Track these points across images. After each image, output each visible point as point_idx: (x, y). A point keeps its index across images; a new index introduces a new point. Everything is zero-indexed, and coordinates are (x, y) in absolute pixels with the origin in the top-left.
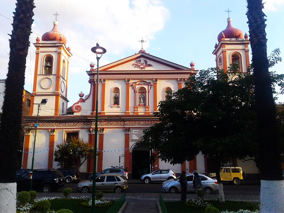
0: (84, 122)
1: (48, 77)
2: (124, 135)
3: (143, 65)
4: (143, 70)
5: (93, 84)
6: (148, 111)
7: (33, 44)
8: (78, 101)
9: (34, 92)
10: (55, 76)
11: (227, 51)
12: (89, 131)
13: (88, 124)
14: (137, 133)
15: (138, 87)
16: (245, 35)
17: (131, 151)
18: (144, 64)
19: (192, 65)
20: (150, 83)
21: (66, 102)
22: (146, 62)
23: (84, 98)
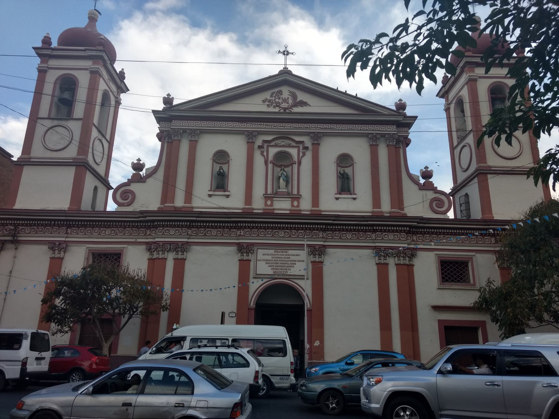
1: (63, 123)
2: (238, 263)
4: (287, 111)
5: (167, 142)
6: (298, 206)
7: (34, 48)
8: (128, 180)
9: (24, 156)
10: (80, 123)
11: (478, 79)
12: (149, 250)
13: (148, 233)
14: (269, 257)
15: (273, 151)
17: (252, 304)
18: (290, 101)
20: (302, 142)
21: (105, 189)
22: (294, 96)
23: (143, 173)
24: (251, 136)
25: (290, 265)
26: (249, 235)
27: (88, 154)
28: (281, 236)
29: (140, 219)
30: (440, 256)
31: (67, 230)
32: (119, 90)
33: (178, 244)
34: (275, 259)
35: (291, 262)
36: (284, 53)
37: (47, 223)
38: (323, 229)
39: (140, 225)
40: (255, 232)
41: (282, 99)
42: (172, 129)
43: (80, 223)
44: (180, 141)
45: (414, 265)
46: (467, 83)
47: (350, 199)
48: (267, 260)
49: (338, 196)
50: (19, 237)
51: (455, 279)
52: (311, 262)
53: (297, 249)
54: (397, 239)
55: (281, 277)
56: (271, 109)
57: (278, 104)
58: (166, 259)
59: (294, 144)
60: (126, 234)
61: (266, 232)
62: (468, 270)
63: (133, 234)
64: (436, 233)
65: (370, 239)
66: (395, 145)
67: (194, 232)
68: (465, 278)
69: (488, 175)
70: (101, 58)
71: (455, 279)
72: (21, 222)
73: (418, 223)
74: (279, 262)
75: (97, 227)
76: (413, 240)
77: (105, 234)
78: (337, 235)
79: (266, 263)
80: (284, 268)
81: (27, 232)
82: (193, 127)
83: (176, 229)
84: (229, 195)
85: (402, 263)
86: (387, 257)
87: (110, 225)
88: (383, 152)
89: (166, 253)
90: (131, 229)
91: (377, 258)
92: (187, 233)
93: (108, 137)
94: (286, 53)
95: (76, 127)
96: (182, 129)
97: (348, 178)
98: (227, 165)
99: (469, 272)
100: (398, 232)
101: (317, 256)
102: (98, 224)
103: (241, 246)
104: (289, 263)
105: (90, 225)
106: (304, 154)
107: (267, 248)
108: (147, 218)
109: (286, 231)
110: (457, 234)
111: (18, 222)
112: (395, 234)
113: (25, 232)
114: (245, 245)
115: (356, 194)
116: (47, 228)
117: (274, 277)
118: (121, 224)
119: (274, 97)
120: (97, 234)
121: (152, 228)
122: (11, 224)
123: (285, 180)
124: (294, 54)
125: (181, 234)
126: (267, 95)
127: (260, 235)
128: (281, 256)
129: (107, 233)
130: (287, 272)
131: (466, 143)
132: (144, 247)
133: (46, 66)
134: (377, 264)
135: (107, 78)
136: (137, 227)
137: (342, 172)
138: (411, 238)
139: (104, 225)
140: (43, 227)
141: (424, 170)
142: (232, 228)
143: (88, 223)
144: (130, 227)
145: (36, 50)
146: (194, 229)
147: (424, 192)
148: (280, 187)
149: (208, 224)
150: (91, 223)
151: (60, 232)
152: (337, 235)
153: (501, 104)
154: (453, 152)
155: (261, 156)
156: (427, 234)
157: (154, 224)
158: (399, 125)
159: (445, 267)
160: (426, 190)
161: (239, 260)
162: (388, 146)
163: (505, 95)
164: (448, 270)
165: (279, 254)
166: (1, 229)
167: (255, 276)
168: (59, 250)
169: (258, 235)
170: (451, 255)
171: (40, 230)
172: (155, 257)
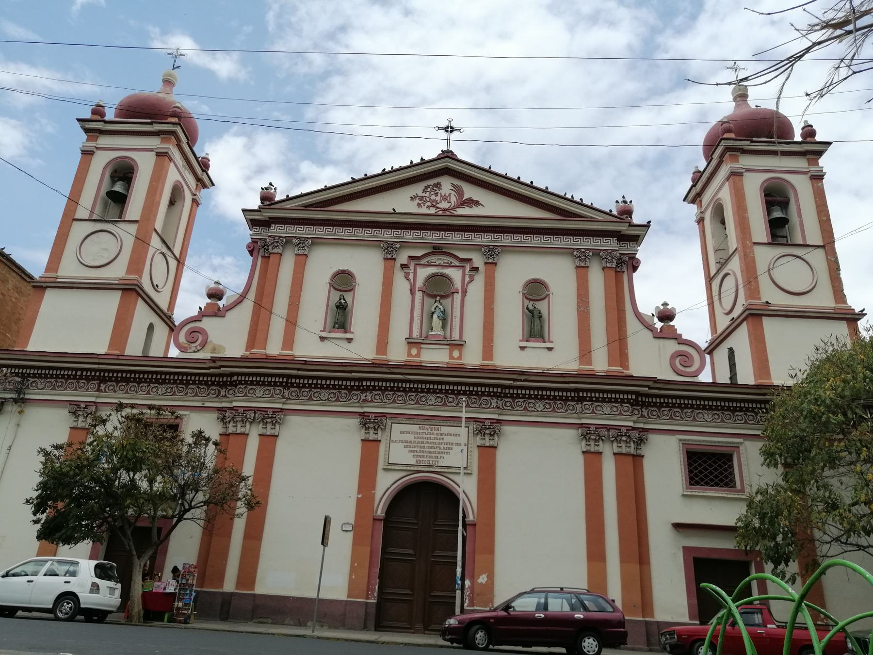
0: (208, 386)
2: (359, 445)
3: (449, 202)
4: (448, 213)
5: (262, 257)
6: (460, 358)
7: (79, 120)
10: (133, 229)
11: (745, 174)
13: (223, 393)
14: (410, 437)
15: (423, 273)
16: (803, 129)
17: (379, 513)
18: (453, 199)
19: (626, 212)
20: (469, 260)
21: (167, 329)
22: (459, 192)
23: (221, 304)
24: (390, 250)
25: (444, 451)
26: (378, 401)
27: (142, 272)
28: (431, 403)
29: (212, 370)
30: (686, 442)
31: (99, 386)
32: (199, 184)
33: (267, 412)
34: (420, 440)
35: (445, 446)
36: (446, 129)
37: (70, 373)
38: (498, 394)
39: (211, 381)
40: (389, 396)
41: (441, 196)
42: (269, 236)
43: (120, 375)
44: (281, 255)
45: (643, 456)
46: (728, 179)
47: (542, 349)
48: (406, 442)
49: (524, 344)
50: (28, 394)
51: (712, 480)
52: (478, 446)
53: (455, 425)
54: (617, 413)
55: (427, 469)
56: (424, 210)
57: (434, 203)
58: (248, 435)
59: (458, 264)
60: (189, 394)
61: (406, 396)
62: (731, 467)
63: (200, 395)
64: (680, 406)
65: (574, 412)
66: (615, 268)
67: (294, 394)
68: (727, 480)
69: (763, 317)
70: (173, 133)
71: (712, 480)
72: (32, 371)
73: (650, 388)
74: (426, 445)
75: (145, 382)
76: (643, 416)
77: (157, 393)
78: (520, 404)
79: (405, 447)
80: (434, 455)
81: (40, 386)
82: (303, 234)
83: (266, 388)
84: (352, 339)
85: (624, 452)
86: (601, 442)
87: (165, 379)
88: (597, 278)
89: (248, 424)
90: (198, 387)
91: (584, 442)
92: (283, 395)
93: (177, 252)
94: (449, 129)
95: (127, 233)
96: (285, 237)
97: (541, 317)
98: (351, 293)
99: (733, 470)
100: (618, 402)
101: (487, 437)
102: (148, 378)
103: (366, 418)
104: (442, 446)
105: (135, 378)
106: (472, 279)
107: (408, 422)
108: (222, 369)
109: (439, 395)
110: (714, 407)
111: (28, 372)
112: (614, 404)
113: (37, 387)
114: (372, 417)
115: (552, 342)
116: (69, 381)
117: (416, 469)
118: (182, 377)
119: (428, 193)
120: (145, 393)
121: (229, 386)
122: (17, 375)
123: (440, 318)
124: (462, 131)
125: (272, 396)
126: (417, 189)
127: (398, 402)
128: (430, 436)
129: (160, 392)
130: (438, 462)
131: (730, 270)
132: (214, 416)
133: (95, 145)
134: (584, 452)
135: (181, 164)
136: (206, 384)
137: (531, 308)
138: (639, 412)
139: (156, 379)
140: (63, 381)
141: (662, 307)
142: (352, 388)
143: (133, 376)
144: (196, 384)
145: (81, 123)
146: (293, 389)
147: (661, 341)
148: (432, 329)
149: (315, 382)
150: (137, 376)
151: (88, 389)
152: (520, 404)
153: (782, 211)
154: (711, 284)
155: (405, 280)
156: (666, 407)
157: (232, 380)
158: (622, 238)
159: (695, 462)
160: (664, 338)
161: (362, 440)
162: (604, 268)
163: (786, 197)
164: (700, 465)
165: (427, 431)
166: (2, 381)
167: (386, 467)
168: (85, 415)
169: (394, 402)
170: (704, 441)
171: (60, 384)
172: (230, 431)
